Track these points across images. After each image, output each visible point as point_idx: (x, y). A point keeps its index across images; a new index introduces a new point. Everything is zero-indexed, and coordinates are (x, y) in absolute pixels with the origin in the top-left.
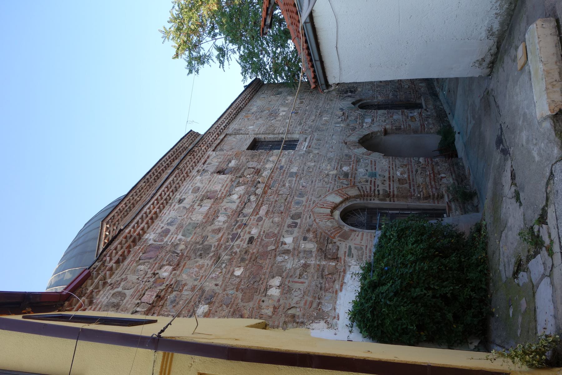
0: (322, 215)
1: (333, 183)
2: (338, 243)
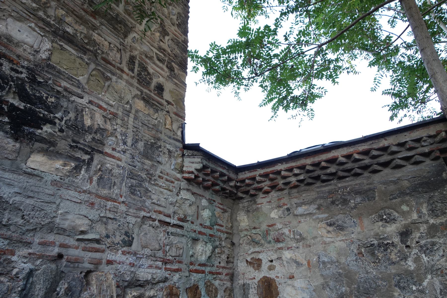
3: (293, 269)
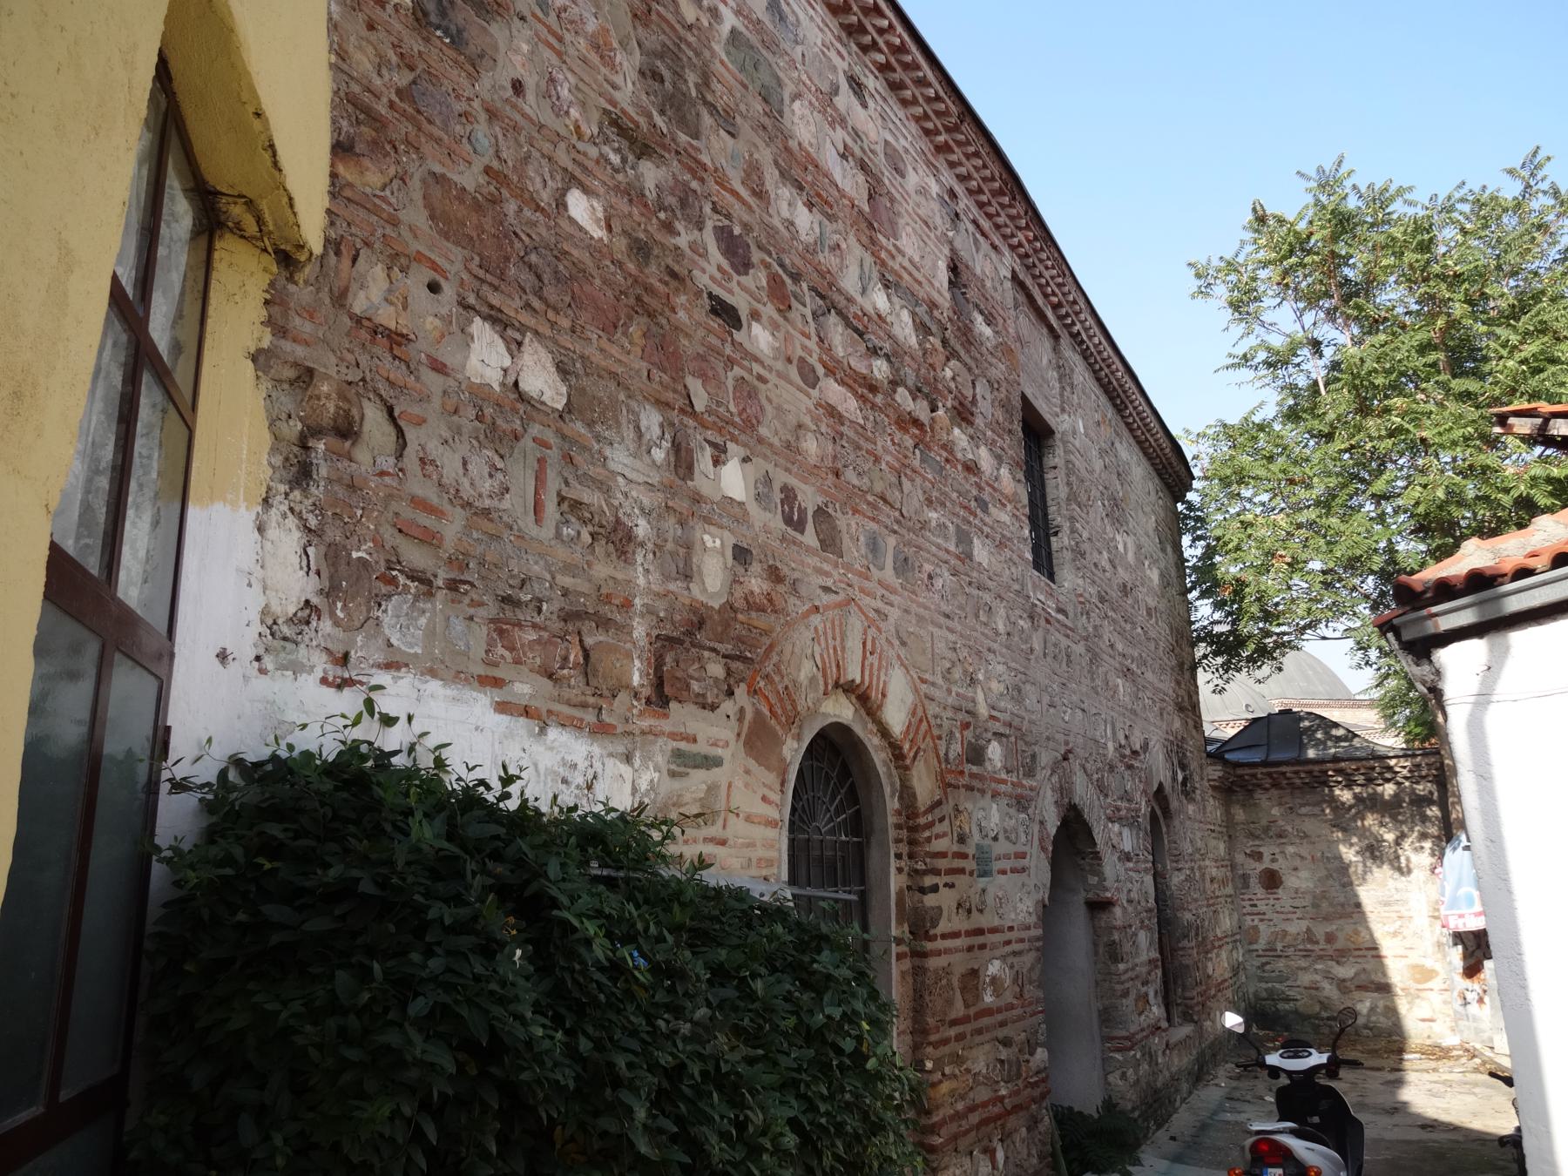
0: (838, 642)
1: (950, 700)
2: (728, 706)
3: (1298, 862)
